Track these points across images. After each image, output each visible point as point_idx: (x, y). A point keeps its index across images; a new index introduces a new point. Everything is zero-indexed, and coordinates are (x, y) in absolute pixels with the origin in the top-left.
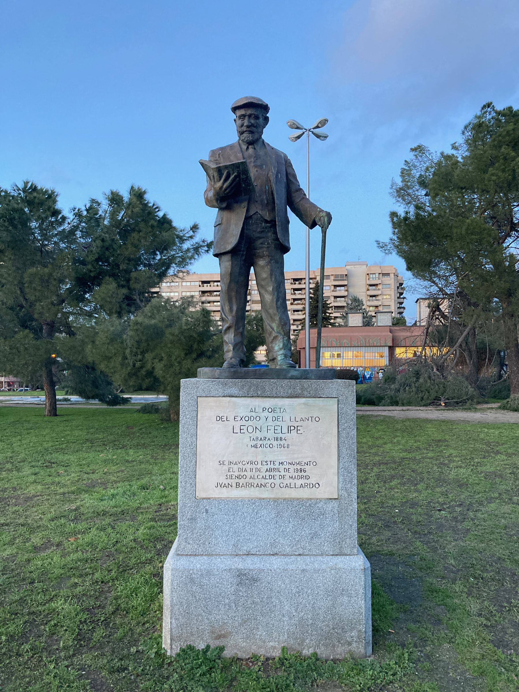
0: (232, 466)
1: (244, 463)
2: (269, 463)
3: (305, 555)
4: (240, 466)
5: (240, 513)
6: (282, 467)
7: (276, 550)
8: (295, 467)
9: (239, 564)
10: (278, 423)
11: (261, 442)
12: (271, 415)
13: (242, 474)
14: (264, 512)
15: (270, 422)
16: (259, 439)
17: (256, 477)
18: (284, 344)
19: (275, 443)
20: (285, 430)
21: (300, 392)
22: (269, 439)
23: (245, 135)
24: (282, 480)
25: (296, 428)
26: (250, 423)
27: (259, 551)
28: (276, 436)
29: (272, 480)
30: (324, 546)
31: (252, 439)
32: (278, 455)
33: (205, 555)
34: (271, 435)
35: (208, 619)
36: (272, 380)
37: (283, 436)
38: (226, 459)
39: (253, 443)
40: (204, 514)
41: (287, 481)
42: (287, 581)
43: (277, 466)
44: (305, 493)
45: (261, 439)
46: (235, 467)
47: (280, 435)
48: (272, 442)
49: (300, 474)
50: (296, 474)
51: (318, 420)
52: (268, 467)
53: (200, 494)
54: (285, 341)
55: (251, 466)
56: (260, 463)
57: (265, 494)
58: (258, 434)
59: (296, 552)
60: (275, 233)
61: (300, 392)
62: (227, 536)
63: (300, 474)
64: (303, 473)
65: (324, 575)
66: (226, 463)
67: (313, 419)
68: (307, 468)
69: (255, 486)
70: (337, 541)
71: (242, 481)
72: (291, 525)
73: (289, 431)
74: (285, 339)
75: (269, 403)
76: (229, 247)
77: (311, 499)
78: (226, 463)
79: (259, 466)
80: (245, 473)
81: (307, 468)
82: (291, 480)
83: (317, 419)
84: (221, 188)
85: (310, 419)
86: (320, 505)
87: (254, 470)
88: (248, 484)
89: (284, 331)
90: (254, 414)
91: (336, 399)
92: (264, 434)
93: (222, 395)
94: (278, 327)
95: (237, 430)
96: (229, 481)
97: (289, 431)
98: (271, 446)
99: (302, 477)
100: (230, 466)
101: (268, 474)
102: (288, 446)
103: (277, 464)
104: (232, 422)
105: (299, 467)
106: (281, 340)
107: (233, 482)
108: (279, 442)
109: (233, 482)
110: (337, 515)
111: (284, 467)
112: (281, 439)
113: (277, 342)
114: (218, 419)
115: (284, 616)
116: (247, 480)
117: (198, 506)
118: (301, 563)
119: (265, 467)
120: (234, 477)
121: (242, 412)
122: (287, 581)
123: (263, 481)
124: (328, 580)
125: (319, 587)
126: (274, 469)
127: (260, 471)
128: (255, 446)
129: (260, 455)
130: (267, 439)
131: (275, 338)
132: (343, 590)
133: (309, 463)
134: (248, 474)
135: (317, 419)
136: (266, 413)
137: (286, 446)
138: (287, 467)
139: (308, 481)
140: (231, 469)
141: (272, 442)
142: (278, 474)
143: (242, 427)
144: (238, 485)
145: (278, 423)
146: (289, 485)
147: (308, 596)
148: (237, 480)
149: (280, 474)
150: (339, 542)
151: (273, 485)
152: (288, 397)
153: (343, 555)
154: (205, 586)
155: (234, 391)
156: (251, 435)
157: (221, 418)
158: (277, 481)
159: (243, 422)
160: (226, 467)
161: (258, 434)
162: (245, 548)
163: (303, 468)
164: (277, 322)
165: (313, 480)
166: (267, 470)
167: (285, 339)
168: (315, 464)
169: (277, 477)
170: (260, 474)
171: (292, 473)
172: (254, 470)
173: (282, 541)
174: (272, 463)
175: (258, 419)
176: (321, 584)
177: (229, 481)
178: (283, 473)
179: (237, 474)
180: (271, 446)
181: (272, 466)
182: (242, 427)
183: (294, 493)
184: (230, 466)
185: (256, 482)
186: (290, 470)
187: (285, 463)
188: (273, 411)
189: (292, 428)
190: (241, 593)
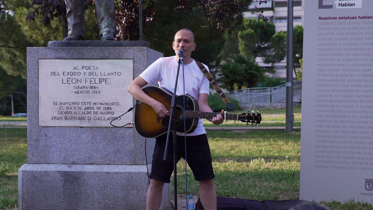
0: (62, 105)
1: (70, 103)
2: (87, 103)
3: (111, 165)
4: (68, 105)
5: (68, 137)
6: (95, 106)
7: (92, 161)
8: (104, 106)
9: (65, 168)
10: (93, 77)
11: (81, 90)
12: (88, 71)
13: (69, 111)
14: (83, 136)
15: (87, 76)
16: (80, 88)
17: (78, 113)
18: (108, 24)
19: (91, 90)
20: (97, 81)
21: (108, 55)
22: (87, 88)
24: (95, 115)
25: (105, 80)
26: (74, 77)
27: (81, 162)
28: (92, 85)
29: (89, 115)
30: (123, 158)
31: (75, 88)
32: (93, 99)
33: (45, 164)
34: (88, 84)
35: (46, 203)
36: (89, 47)
37: (96, 85)
38: (58, 101)
39: (76, 90)
40: (44, 137)
41: (99, 116)
42: (97, 179)
43: (92, 106)
45: (81, 88)
46: (64, 107)
47: (94, 85)
48: (89, 89)
49: (108, 111)
50: (105, 111)
51: (119, 74)
52: (86, 106)
53: (42, 124)
54: (109, 21)
55: (75, 106)
56: (81, 103)
57: (85, 124)
58: (80, 84)
59: (105, 162)
61: (108, 55)
62: (59, 151)
63: (108, 111)
64: (109, 110)
65: (121, 176)
66: (58, 103)
67: (117, 73)
68: (112, 107)
69: (78, 119)
70: (133, 155)
71: (68, 116)
72: (101, 145)
73: (100, 81)
74: (109, 20)
75: (86, 63)
78: (58, 103)
79: (80, 106)
80: (71, 110)
81: (112, 107)
82: (102, 115)
83: (119, 74)
85: (114, 74)
86: (121, 132)
87: (77, 108)
88: (73, 117)
89: (108, 13)
90: (77, 71)
91: (132, 60)
93: (55, 58)
94: (104, 11)
95: (65, 81)
96: (60, 115)
97: (100, 81)
98: (88, 92)
99: (109, 113)
100: (61, 106)
101: (86, 111)
102: (99, 92)
103: (92, 104)
104: (62, 76)
105: (107, 106)
106: (106, 21)
107: (63, 116)
108: (93, 90)
109: (63, 116)
110: (132, 138)
111: (97, 106)
112: (95, 87)
113: (103, 22)
114: (52, 74)
115: (95, 202)
116: (72, 115)
117: (40, 132)
118: (106, 169)
119: (84, 107)
120: (63, 113)
121: (71, 70)
122: (97, 179)
123: (83, 116)
124: (123, 179)
125: (118, 183)
126: (90, 108)
127: (80, 109)
128: (77, 92)
129: (80, 98)
130: (85, 88)
131: (103, 19)
132: (133, 186)
133: (113, 103)
134: (73, 111)
135: (119, 74)
136: (85, 70)
137: (98, 92)
138: (99, 106)
139: (113, 116)
140: (62, 108)
141: (89, 89)
142: (92, 111)
143: (68, 80)
144: (66, 118)
145: (93, 77)
146: (100, 118)
147: (111, 189)
148: (66, 115)
149: (94, 111)
150: (134, 156)
151: (89, 118)
152: (100, 59)
153: (135, 165)
154: (44, 182)
155: (63, 54)
156: (74, 85)
157: (54, 73)
159: (69, 76)
160: (58, 107)
162: (71, 160)
163: (109, 106)
164: (103, 7)
166: (85, 108)
167: (109, 20)
168: (117, 104)
169: (92, 113)
170: (81, 111)
171: (102, 110)
172: (77, 108)
173: (95, 156)
174: (89, 103)
175: (79, 73)
176: (119, 182)
177: (60, 115)
178: (96, 110)
179: (65, 110)
180: (88, 92)
181: (89, 106)
182: (68, 80)
184: (61, 106)
185: (78, 116)
186: (101, 109)
187: (98, 104)
189: (102, 80)
190: (67, 187)
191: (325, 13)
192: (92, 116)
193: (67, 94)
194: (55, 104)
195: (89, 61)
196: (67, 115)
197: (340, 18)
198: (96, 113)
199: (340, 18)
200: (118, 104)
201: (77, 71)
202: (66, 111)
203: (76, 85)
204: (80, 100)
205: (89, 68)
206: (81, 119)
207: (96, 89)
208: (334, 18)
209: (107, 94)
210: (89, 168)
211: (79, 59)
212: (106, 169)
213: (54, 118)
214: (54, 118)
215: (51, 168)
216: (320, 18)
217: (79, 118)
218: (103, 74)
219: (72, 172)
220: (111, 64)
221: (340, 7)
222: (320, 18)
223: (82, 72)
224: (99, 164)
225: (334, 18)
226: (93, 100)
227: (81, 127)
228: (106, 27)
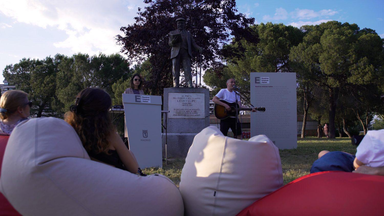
4: (179, 110)
6: (190, 111)
12: (187, 97)
19: (188, 104)
20: (191, 101)
23: (180, 28)
25: (194, 101)
26: (182, 99)
28: (189, 103)
32: (189, 108)
34: (187, 102)
41: (192, 114)
44: (196, 117)
46: (178, 111)
52: (187, 110)
57: (186, 117)
58: (184, 102)
60: (188, 53)
68: (197, 111)
71: (180, 114)
73: (192, 101)
75: (187, 94)
76: (175, 56)
77: (198, 119)
79: (184, 110)
81: (197, 111)
84: (174, 40)
90: (183, 97)
92: (186, 102)
94: (189, 78)
95: (179, 101)
102: (192, 105)
104: (177, 99)
105: (195, 111)
112: (190, 103)
126: (188, 111)
127: (184, 111)
128: (183, 105)
129: (184, 107)
134: (182, 112)
136: (186, 97)
138: (192, 110)
141: (188, 104)
144: (179, 115)
155: (178, 91)
158: (189, 114)
159: (180, 99)
160: (176, 111)
161: (184, 102)
165: (198, 114)
179: (179, 112)
181: (188, 110)
183: (193, 117)
185: (183, 114)
188: (188, 96)
191: (257, 85)
192: (189, 114)
193: (179, 106)
194: (175, 109)
195: (188, 94)
196: (179, 114)
197: (262, 87)
198: (191, 113)
199: (262, 87)
200: (199, 110)
201: (183, 97)
202: (179, 112)
203: (183, 102)
204: (185, 108)
205: (188, 96)
206: (185, 115)
207: (191, 104)
208: (260, 87)
209: (195, 106)
211: (184, 93)
213: (174, 115)
214: (174, 115)
215: (173, 134)
216: (256, 87)
217: (184, 115)
218: (193, 98)
219: (182, 136)
220: (196, 95)
221: (262, 83)
222: (256, 87)
223: (185, 97)
224: (192, 133)
225: (260, 87)
226: (190, 108)
227: (185, 119)
228: (189, 84)
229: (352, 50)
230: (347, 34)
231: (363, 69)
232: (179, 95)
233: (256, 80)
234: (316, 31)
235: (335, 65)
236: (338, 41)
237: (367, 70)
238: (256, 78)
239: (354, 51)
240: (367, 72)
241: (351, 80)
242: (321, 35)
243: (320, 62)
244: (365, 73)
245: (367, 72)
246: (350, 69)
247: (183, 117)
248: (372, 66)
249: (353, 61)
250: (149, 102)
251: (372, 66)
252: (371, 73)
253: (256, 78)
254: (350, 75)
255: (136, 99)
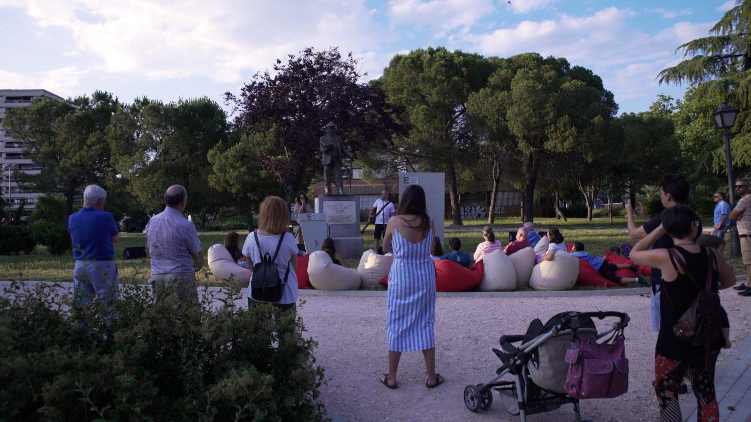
44: (349, 223)
51: (351, 206)
75: (340, 202)
118: (348, 238)
210: (342, 238)
212: (348, 238)
229: (551, 104)
230: (547, 78)
231: (563, 132)
232: (333, 203)
233: (405, 180)
234: (505, 70)
235: (526, 125)
236: (532, 90)
237: (567, 134)
238: (405, 178)
239: (553, 105)
240: (568, 137)
241: (549, 145)
242: (513, 77)
243: (507, 118)
244: (565, 139)
245: (568, 137)
246: (546, 132)
247: (337, 223)
248: (573, 129)
249: (551, 120)
250: (318, 218)
251: (573, 129)
252: (574, 138)
253: (405, 178)
254: (547, 139)
255: (308, 217)
